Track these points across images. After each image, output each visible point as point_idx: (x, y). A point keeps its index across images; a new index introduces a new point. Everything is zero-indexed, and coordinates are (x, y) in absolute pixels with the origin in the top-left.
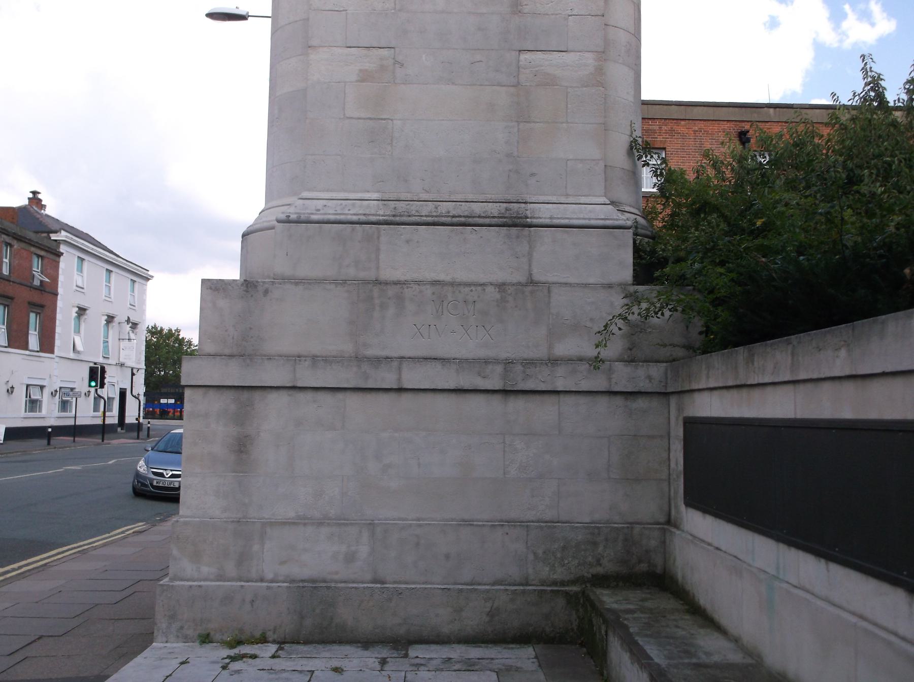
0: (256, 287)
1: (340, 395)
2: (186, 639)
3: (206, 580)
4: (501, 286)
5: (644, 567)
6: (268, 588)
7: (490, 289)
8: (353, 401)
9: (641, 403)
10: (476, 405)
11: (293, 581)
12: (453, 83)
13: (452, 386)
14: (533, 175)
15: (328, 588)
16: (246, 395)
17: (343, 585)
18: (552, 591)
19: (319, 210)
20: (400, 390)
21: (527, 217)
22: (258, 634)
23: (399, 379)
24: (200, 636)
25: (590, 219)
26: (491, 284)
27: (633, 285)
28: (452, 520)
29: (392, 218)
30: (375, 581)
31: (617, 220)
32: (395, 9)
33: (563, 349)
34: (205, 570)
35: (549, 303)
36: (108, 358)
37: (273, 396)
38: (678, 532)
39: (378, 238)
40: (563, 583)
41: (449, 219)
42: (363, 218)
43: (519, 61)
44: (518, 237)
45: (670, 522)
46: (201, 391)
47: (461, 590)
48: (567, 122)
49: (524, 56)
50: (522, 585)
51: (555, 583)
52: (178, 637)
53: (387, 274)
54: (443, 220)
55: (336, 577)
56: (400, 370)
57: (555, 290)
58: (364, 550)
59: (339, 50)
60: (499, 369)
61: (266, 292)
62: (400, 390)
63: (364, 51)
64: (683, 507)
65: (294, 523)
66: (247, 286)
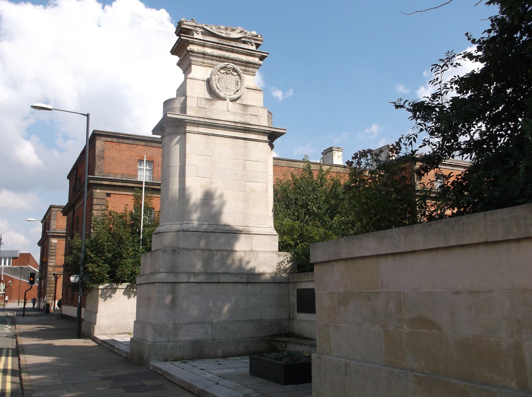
0: (176, 251)
1: (202, 284)
2: (160, 361)
3: (165, 342)
4: (245, 252)
5: (284, 332)
6: (184, 343)
7: (242, 253)
8: (205, 286)
9: (282, 285)
10: (240, 286)
11: (189, 341)
12: (228, 190)
13: (233, 281)
14: (250, 218)
15: (201, 342)
16: (174, 285)
17: (205, 341)
18: (262, 340)
19: (191, 227)
20: (219, 283)
21: (250, 231)
22: (181, 358)
23: (219, 279)
24: (164, 359)
25: (267, 232)
26: (242, 251)
27: (279, 251)
28: (234, 321)
29: (213, 231)
30: (213, 340)
31: (274, 233)
32: (211, 166)
34: (164, 339)
35: (257, 257)
36: (314, 281)
37: (182, 285)
38: (295, 320)
39: (210, 236)
40: (263, 337)
41: (229, 231)
42: (205, 230)
43: (245, 184)
44: (248, 237)
45: (290, 319)
46: (161, 284)
47: (238, 341)
48: (259, 203)
49: (247, 183)
50: (253, 338)
51: (261, 337)
52: (157, 360)
55: (202, 339)
56: (219, 276)
57: (259, 253)
58: (210, 331)
59: (194, 177)
60: (246, 276)
61: (179, 253)
62: (219, 283)
63: (202, 178)
64: (296, 314)
65: (190, 324)
66: (173, 251)
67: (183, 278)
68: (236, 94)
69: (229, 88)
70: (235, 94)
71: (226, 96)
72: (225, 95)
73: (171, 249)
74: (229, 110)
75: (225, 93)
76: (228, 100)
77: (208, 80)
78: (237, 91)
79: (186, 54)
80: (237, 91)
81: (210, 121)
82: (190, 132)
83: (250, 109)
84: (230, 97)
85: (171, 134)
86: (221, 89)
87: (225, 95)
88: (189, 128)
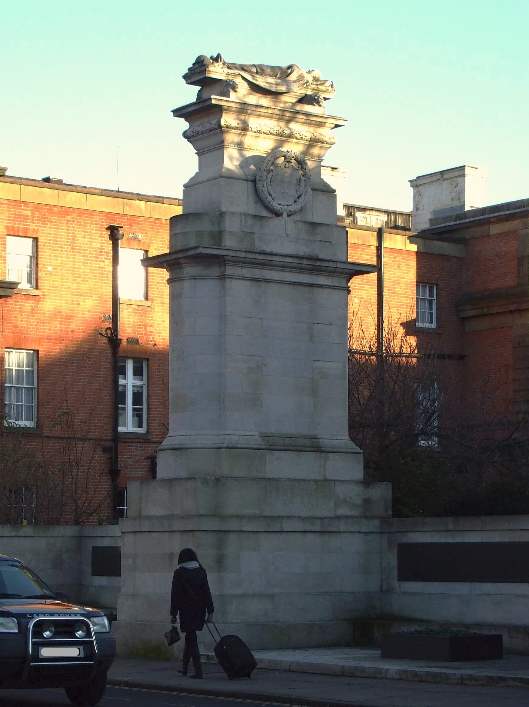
13: (301, 530)
21: (322, 447)
23: (282, 527)
29: (269, 447)
33: (341, 512)
42: (258, 447)
53: (269, 475)
54: (291, 448)
64: (396, 584)
67: (233, 525)
68: (298, 203)
69: (287, 192)
70: (295, 202)
71: (282, 207)
72: (280, 205)
73: (213, 479)
74: (288, 234)
75: (279, 203)
76: (285, 215)
77: (253, 178)
78: (299, 198)
79: (215, 129)
80: (299, 198)
81: (262, 257)
82: (232, 277)
83: (319, 230)
84: (288, 210)
85: (196, 278)
86: (274, 196)
87: (280, 205)
88: (230, 270)
